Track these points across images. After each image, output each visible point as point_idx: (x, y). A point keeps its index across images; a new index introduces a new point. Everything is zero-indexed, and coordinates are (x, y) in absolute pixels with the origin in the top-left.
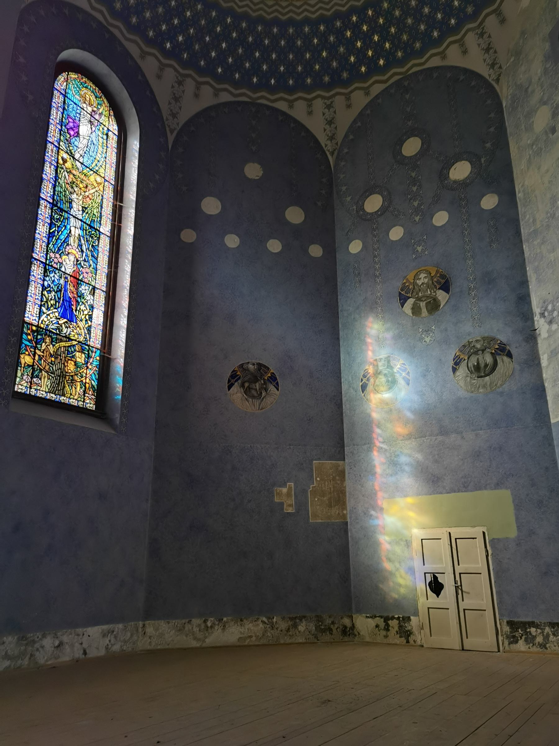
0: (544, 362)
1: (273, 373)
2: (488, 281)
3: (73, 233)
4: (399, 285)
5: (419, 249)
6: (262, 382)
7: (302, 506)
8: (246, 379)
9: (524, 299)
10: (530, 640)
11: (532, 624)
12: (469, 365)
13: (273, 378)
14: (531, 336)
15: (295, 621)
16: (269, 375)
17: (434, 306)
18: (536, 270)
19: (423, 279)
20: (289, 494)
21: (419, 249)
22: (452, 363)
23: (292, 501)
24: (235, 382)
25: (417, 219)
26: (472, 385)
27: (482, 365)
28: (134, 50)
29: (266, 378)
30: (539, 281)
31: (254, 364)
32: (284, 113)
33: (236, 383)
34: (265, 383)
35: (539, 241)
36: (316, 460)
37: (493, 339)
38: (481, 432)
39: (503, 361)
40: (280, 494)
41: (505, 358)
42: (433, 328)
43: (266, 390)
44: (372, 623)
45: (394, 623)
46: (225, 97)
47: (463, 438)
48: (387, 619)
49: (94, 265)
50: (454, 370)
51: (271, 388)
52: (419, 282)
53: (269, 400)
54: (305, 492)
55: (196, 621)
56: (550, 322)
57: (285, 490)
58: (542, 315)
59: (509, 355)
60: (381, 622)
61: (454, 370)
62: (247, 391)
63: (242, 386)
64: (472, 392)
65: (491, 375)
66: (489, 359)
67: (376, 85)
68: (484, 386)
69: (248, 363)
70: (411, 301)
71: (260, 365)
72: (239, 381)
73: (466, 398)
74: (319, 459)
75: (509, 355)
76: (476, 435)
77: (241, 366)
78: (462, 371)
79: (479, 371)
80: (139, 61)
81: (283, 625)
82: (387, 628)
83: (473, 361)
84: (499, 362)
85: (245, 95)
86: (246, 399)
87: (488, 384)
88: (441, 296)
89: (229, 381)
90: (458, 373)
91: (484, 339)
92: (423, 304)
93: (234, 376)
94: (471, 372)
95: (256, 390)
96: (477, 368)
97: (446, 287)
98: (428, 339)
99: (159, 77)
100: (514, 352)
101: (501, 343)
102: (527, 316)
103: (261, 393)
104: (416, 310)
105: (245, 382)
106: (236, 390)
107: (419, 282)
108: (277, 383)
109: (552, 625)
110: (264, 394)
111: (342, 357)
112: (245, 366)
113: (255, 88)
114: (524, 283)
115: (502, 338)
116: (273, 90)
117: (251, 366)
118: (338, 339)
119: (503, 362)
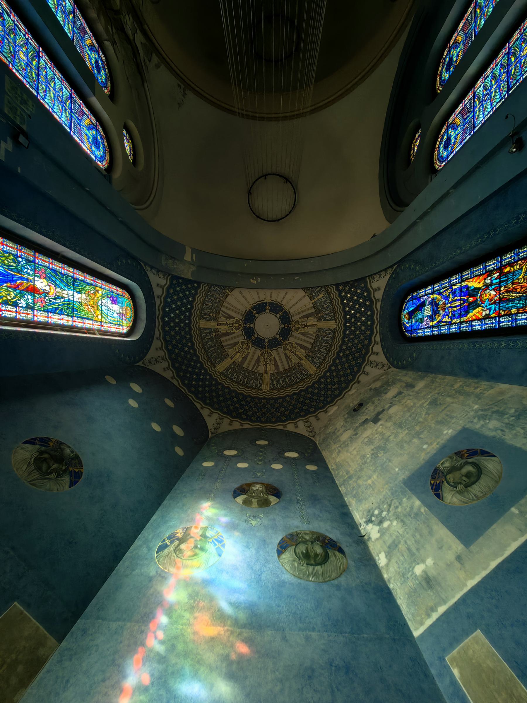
1: (82, 473)
3: (64, 292)
6: (63, 468)
8: (51, 452)
12: (297, 551)
16: (77, 470)
24: (38, 445)
25: (260, 463)
26: (300, 571)
27: (312, 555)
28: (157, 334)
29: (70, 469)
31: (72, 452)
33: (38, 446)
34: (65, 471)
35: (354, 480)
36: (22, 603)
38: (314, 635)
41: (337, 553)
42: (262, 516)
43: (59, 475)
47: (284, 639)
49: (51, 310)
51: (66, 479)
63: (41, 453)
64: (300, 578)
65: (323, 566)
67: (248, 425)
69: (70, 447)
71: (77, 457)
72: (43, 448)
73: (291, 584)
74: (28, 606)
76: (307, 638)
79: (307, 558)
80: (155, 338)
83: (302, 548)
84: (330, 554)
86: (29, 463)
87: (320, 573)
89: (35, 439)
90: (283, 556)
93: (44, 441)
94: (299, 558)
95: (49, 467)
100: (345, 549)
103: (51, 473)
105: (49, 454)
106: (30, 449)
108: (76, 482)
110: (53, 476)
111: (154, 517)
112: (62, 446)
117: (68, 451)
118: (159, 504)
119: (335, 556)
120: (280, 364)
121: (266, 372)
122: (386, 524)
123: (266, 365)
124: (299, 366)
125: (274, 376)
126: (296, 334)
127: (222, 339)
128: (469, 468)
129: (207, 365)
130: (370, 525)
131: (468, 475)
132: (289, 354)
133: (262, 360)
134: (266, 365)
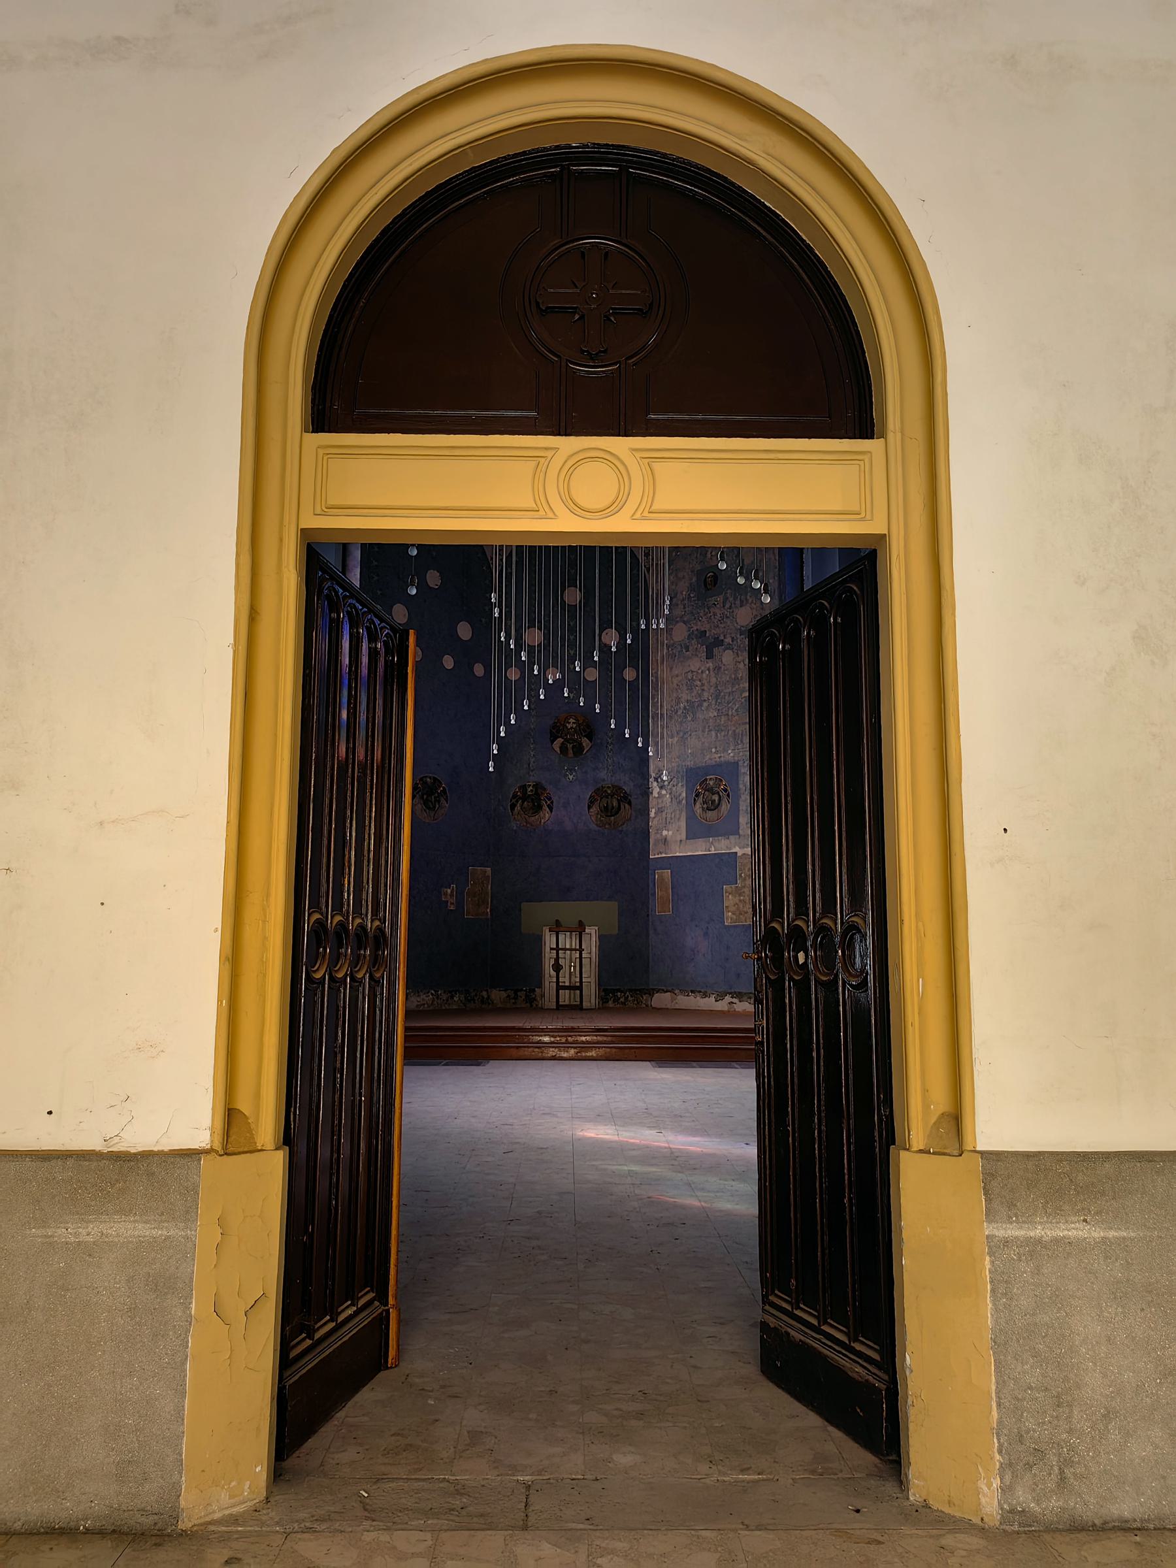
0: (652, 814)
10: (616, 1000)
11: (619, 990)
14: (646, 793)
17: (578, 750)
19: (571, 724)
20: (452, 895)
23: (454, 900)
37: (620, 788)
40: (446, 894)
44: (504, 994)
45: (522, 994)
48: (516, 992)
56: (661, 788)
58: (656, 779)
59: (630, 803)
63: (422, 797)
66: (615, 804)
70: (560, 740)
71: (435, 779)
75: (630, 803)
81: (445, 997)
82: (516, 998)
88: (586, 742)
92: (570, 746)
96: (606, 808)
102: (646, 776)
104: (563, 749)
122: (664, 792)
128: (716, 798)
130: (655, 784)
131: (713, 801)
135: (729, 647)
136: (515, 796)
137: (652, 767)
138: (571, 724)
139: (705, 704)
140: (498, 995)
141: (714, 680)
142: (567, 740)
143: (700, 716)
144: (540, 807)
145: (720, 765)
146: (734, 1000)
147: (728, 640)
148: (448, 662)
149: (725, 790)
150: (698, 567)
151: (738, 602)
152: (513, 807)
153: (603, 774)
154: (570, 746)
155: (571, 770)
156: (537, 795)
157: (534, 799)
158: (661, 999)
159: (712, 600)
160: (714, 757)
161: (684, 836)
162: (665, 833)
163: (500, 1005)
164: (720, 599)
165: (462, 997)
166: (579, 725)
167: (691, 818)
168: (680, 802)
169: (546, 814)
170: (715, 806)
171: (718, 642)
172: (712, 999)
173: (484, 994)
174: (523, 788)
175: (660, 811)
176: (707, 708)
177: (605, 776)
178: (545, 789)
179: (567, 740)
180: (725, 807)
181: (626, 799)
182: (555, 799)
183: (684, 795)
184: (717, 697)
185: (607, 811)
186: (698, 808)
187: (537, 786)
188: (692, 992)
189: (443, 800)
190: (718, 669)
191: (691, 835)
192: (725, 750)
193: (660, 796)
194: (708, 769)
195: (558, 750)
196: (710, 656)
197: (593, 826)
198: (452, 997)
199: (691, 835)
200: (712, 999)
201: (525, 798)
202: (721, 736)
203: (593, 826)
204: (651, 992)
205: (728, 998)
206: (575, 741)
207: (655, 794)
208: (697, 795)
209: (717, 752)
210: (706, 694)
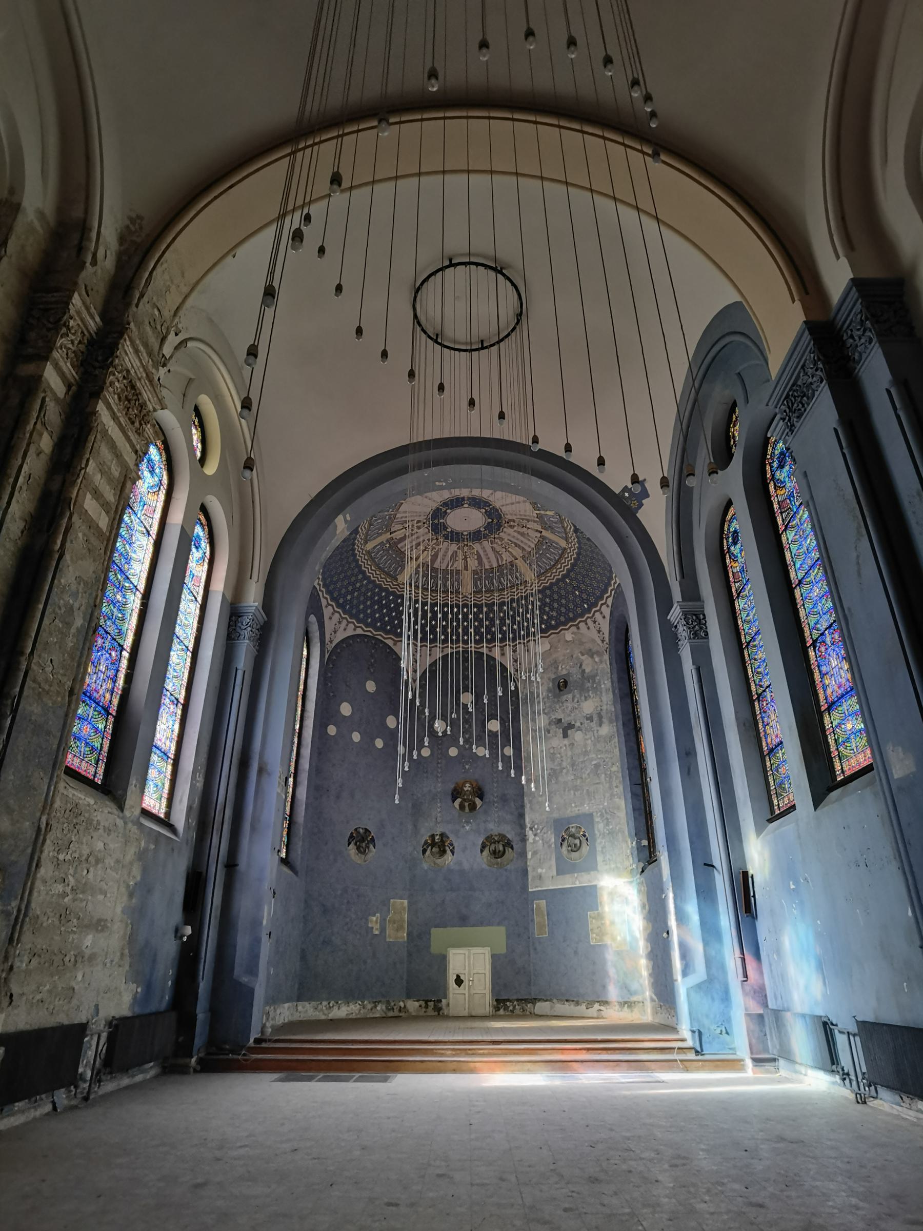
0: (529, 855)
2: (504, 799)
4: (452, 786)
5: (467, 767)
7: (383, 929)
9: (522, 816)
11: (508, 1000)
13: (373, 840)
14: (524, 839)
15: (375, 1004)
17: (473, 807)
18: (530, 802)
19: (467, 787)
20: (376, 922)
21: (467, 767)
22: (479, 847)
30: (531, 809)
32: (390, 648)
39: (508, 850)
40: (372, 921)
44: (417, 1004)
45: (431, 1004)
46: (359, 631)
48: (426, 1002)
50: (482, 851)
51: (371, 846)
52: (466, 789)
53: (370, 855)
54: (385, 920)
55: (325, 1003)
56: (535, 835)
57: (374, 919)
58: (531, 829)
59: (512, 848)
60: (423, 1003)
61: (482, 851)
62: (358, 848)
63: (356, 844)
66: (501, 848)
68: (497, 864)
70: (459, 800)
75: (512, 848)
77: (356, 830)
78: (486, 852)
81: (369, 1006)
82: (427, 1007)
83: (493, 847)
85: (370, 632)
88: (478, 801)
91: (500, 834)
92: (466, 804)
93: (351, 836)
97: (481, 799)
98: (467, 828)
99: (330, 618)
100: (514, 847)
101: (509, 840)
102: (522, 826)
104: (462, 807)
107: (466, 789)
109: (518, 1000)
113: (377, 629)
114: (523, 806)
115: (509, 836)
116: (387, 632)
117: (361, 831)
120: (485, 560)
121: (466, 568)
122: (537, 838)
123: (465, 559)
124: (512, 566)
125: (477, 574)
126: (510, 531)
127: (399, 546)
128: (577, 842)
129: (386, 583)
130: (530, 832)
131: (575, 845)
132: (498, 549)
133: (460, 553)
134: (465, 559)
135: (579, 729)
136: (426, 842)
137: (527, 820)
138: (467, 787)
139: (565, 771)
140: (413, 1005)
141: (569, 753)
142: (464, 800)
143: (560, 779)
144: (444, 852)
145: (578, 816)
146: (602, 1008)
147: (578, 724)
148: (379, 743)
149: (584, 836)
150: (553, 676)
151: (583, 698)
152: (424, 851)
153: (491, 826)
154: (466, 804)
155: (468, 822)
156: (442, 841)
157: (439, 845)
158: (541, 1007)
159: (564, 698)
160: (573, 810)
161: (555, 873)
162: (540, 870)
163: (414, 1014)
164: (570, 696)
165: (384, 1008)
166: (473, 788)
167: (559, 858)
168: (550, 846)
169: (449, 857)
170: (576, 849)
171: (571, 726)
172: (584, 1006)
173: (402, 1004)
174: (433, 836)
175: (535, 853)
176: (566, 773)
177: (494, 828)
178: (448, 838)
179: (464, 800)
180: (585, 849)
181: (509, 844)
182: (455, 845)
183: (553, 840)
184: (573, 765)
185: (496, 854)
186: (565, 848)
187: (442, 835)
188: (567, 1001)
189: (371, 846)
190: (572, 745)
191: (560, 872)
192: (582, 804)
193: (535, 842)
194: (569, 820)
195: (458, 807)
196: (565, 736)
197: (485, 866)
198: (375, 1007)
199: (560, 872)
200: (584, 1006)
201: (433, 844)
202: (578, 793)
203: (485, 866)
204: (534, 1001)
205: (597, 1006)
206: (470, 800)
207: (531, 840)
208: (563, 840)
209: (576, 806)
210: (564, 764)
